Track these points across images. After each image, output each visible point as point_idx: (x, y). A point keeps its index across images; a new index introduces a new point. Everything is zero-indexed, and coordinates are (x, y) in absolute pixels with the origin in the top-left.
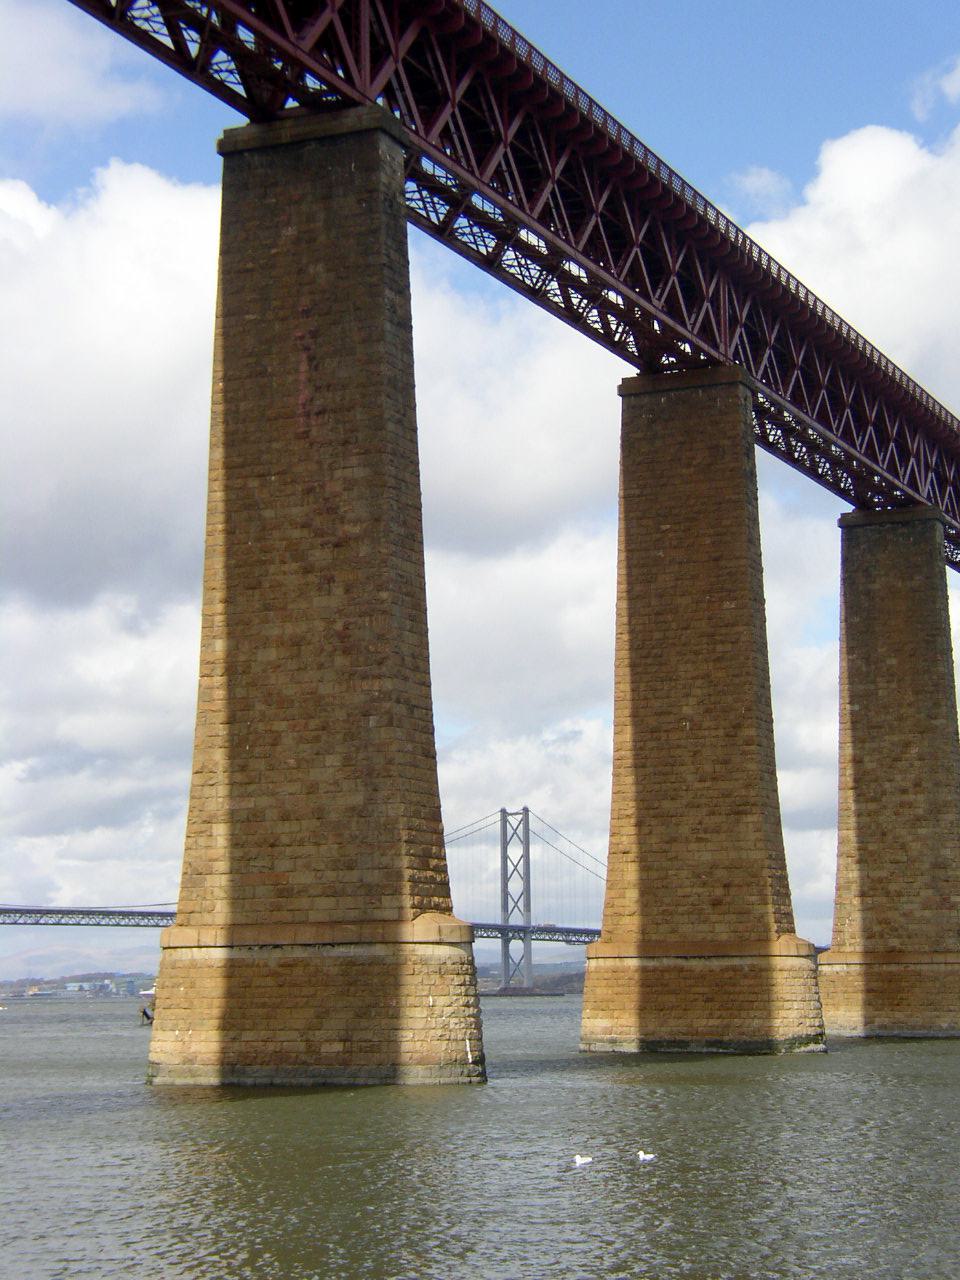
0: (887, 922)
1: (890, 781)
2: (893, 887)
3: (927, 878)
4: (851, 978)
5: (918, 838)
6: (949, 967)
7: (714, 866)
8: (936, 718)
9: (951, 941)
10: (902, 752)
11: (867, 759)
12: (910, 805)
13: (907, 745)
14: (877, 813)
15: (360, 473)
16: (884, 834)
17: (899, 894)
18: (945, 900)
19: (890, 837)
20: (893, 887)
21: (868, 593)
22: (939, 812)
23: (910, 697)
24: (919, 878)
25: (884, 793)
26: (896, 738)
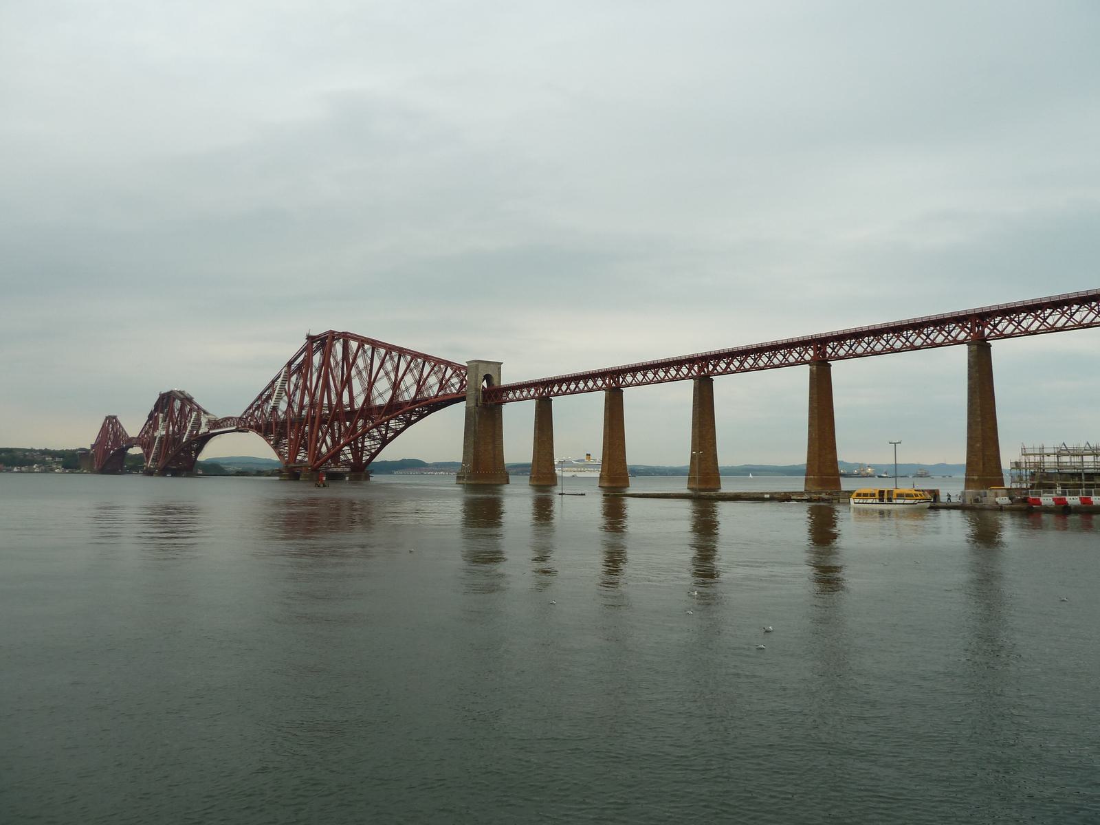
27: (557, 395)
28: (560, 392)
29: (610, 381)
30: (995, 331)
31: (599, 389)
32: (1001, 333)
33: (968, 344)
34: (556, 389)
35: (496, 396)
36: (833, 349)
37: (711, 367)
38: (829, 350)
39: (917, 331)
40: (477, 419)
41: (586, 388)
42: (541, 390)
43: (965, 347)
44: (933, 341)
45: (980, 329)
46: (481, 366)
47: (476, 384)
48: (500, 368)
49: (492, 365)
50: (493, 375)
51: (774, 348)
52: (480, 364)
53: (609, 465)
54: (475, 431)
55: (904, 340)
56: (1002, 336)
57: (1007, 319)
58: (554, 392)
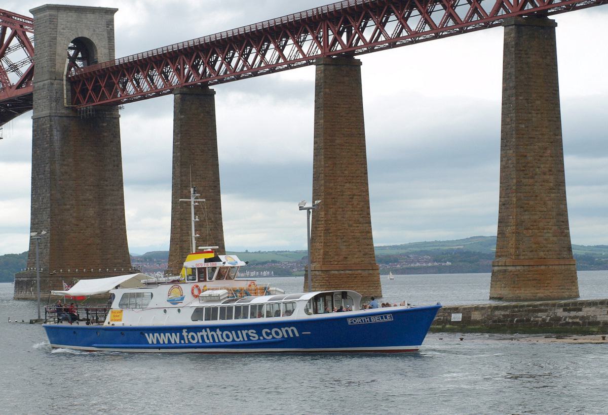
1: (539, 167)
3: (555, 220)
4: (526, 273)
5: (551, 200)
6: (566, 267)
8: (557, 135)
9: (565, 253)
10: (543, 153)
11: (528, 155)
12: (547, 181)
13: (546, 149)
14: (533, 185)
17: (544, 229)
18: (563, 232)
19: (538, 198)
20: (541, 225)
21: (527, 64)
22: (560, 185)
24: (552, 220)
25: (536, 174)
26: (540, 144)
35: (97, 89)
40: (57, 145)
46: (63, 19)
47: (52, 60)
48: (111, 23)
49: (90, 16)
50: (95, 40)
52: (62, 18)
53: (326, 244)
54: (52, 172)
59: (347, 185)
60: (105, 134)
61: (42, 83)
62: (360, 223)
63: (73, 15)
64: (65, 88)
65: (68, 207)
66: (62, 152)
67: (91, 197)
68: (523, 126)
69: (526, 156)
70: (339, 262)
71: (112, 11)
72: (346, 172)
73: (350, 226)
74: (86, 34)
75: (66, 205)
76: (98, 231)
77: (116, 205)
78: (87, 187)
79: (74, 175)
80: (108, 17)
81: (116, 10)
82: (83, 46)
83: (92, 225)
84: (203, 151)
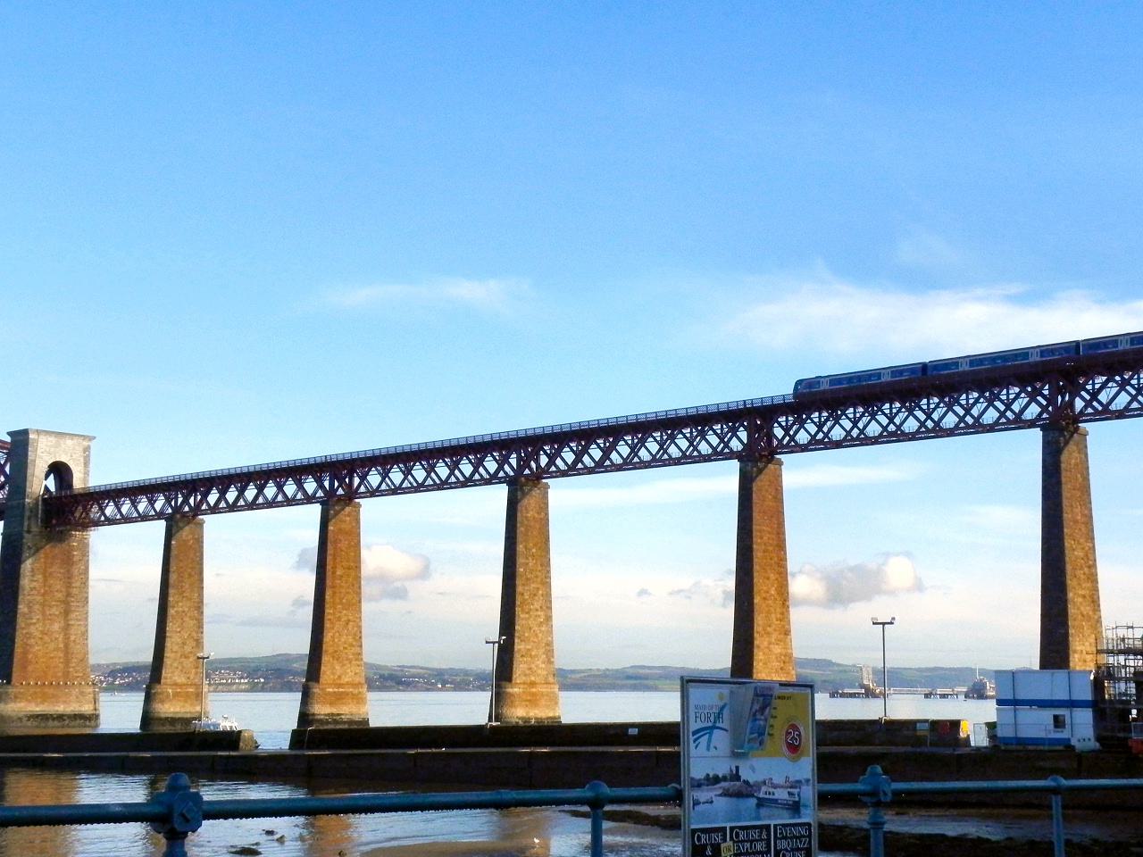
0: (530, 669)
2: (533, 653)
3: (544, 650)
7: (781, 654)
13: (538, 589)
14: (529, 618)
15: (1091, 545)
16: (530, 629)
23: (540, 568)
27: (214, 510)
28: (223, 504)
29: (332, 484)
30: (1095, 403)
31: (309, 499)
32: (1106, 407)
33: (1043, 428)
34: (213, 497)
36: (786, 430)
37: (544, 460)
38: (779, 432)
39: (947, 399)
41: (280, 498)
42: (180, 500)
43: (734, 465)
44: (977, 419)
45: (1067, 398)
48: (87, 449)
51: (670, 424)
55: (922, 417)
56: (1106, 414)
57: (1116, 382)
58: (208, 504)
59: (345, 612)
60: (75, 553)
61: (17, 502)
62: (353, 646)
63: (52, 439)
64: (40, 507)
65: (34, 621)
66: (32, 569)
67: (57, 613)
68: (522, 570)
69: (523, 594)
70: (334, 680)
71: (91, 438)
72: (344, 601)
73: (345, 648)
74: (64, 459)
75: (32, 619)
76: (62, 646)
77: (80, 620)
78: (54, 603)
79: (42, 591)
80: (86, 443)
81: (95, 438)
82: (60, 471)
83: (56, 639)
84: (190, 575)
